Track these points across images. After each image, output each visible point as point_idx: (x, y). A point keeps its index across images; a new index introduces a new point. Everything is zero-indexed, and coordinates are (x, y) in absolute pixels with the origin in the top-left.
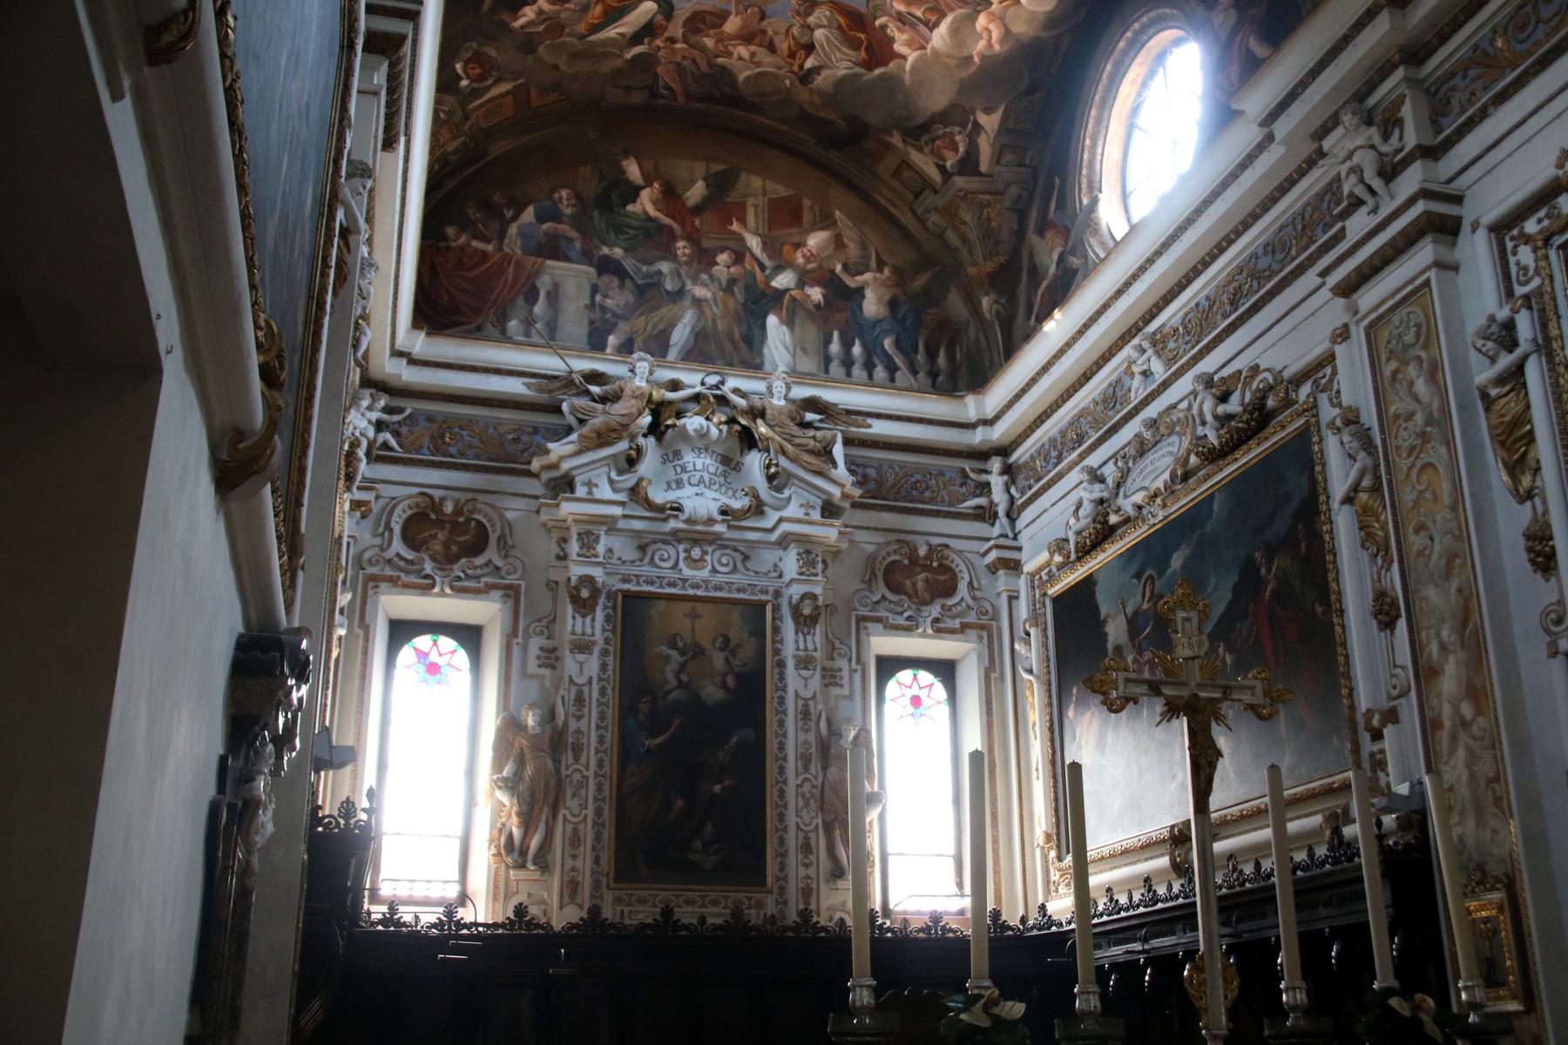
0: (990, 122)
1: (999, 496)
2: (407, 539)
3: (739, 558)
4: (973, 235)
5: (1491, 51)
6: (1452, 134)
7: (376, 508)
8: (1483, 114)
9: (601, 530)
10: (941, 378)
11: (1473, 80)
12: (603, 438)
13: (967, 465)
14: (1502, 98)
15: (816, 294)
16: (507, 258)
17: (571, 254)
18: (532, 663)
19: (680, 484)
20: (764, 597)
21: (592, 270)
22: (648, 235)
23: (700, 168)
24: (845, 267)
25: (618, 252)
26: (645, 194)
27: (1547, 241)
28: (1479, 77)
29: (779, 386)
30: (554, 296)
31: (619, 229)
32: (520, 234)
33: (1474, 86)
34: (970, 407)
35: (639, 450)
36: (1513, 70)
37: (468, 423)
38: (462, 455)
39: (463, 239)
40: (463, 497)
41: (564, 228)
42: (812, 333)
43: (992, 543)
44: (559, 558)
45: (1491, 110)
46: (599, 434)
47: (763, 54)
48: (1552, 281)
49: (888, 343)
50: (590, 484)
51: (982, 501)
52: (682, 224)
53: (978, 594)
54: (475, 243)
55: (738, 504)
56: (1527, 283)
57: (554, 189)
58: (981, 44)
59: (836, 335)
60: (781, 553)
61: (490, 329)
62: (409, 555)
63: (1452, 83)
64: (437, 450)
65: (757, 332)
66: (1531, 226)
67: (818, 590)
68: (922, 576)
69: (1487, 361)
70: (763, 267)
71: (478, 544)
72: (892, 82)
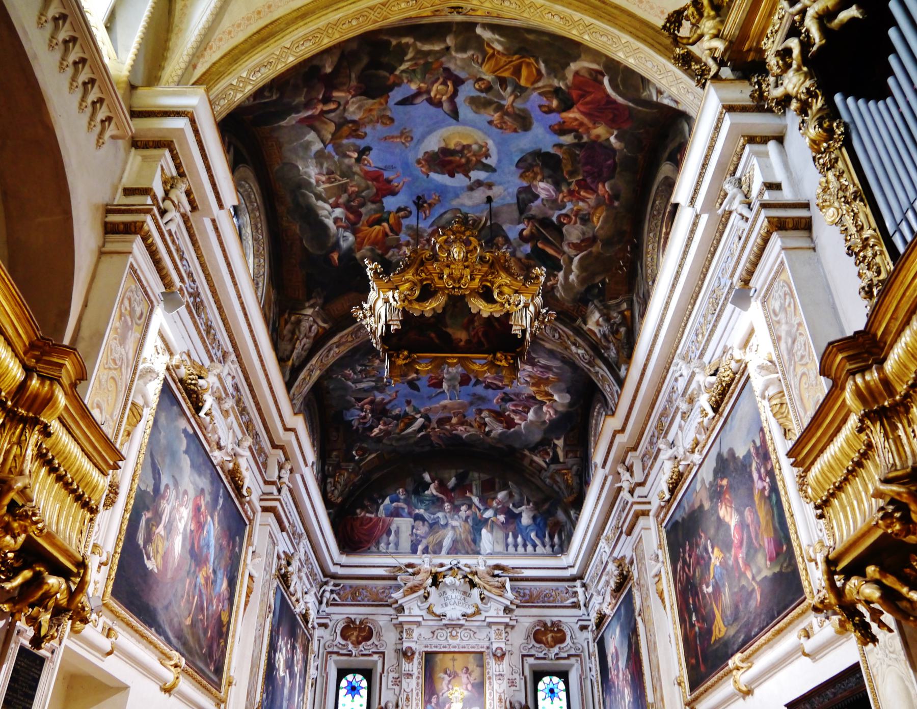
0: (560, 443)
1: (581, 598)
2: (344, 636)
3: (472, 633)
4: (563, 486)
7: (331, 624)
9: (414, 627)
10: (556, 547)
12: (413, 590)
13: (566, 584)
15: (502, 518)
16: (380, 519)
17: (404, 514)
18: (390, 684)
19: (446, 605)
20: (482, 650)
21: (412, 520)
22: (433, 503)
23: (453, 472)
24: (514, 505)
25: (422, 511)
26: (432, 486)
29: (481, 562)
30: (397, 532)
31: (422, 502)
32: (385, 509)
34: (564, 561)
35: (428, 593)
37: (365, 588)
38: (363, 600)
39: (363, 514)
40: (362, 617)
41: (401, 504)
42: (500, 534)
43: (577, 618)
44: (400, 639)
46: (411, 588)
47: (469, 428)
49: (533, 535)
50: (410, 609)
51: (575, 600)
52: (447, 496)
53: (575, 641)
54: (368, 515)
55: (471, 611)
57: (398, 489)
58: (548, 416)
59: (511, 534)
60: (489, 630)
61: (374, 549)
62: (343, 642)
64: (353, 599)
65: (478, 537)
67: (503, 646)
68: (550, 636)
70: (479, 510)
71: (369, 637)
72: (518, 434)
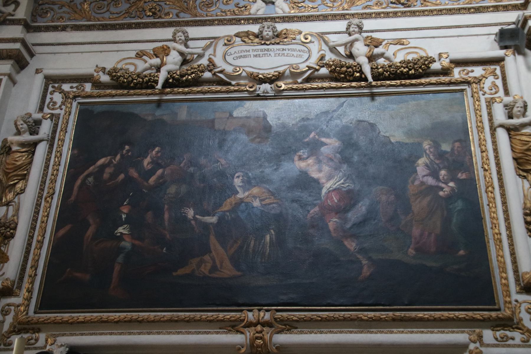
5: (79, 7)
6: (44, 26)
8: (64, 29)
11: (64, 12)
14: (77, 28)
27: (75, 97)
28: (69, 13)
33: (63, 15)
36: (88, 21)
45: (68, 29)
48: (70, 115)
56: (53, 109)
63: (52, 6)
66: (66, 87)
69: (15, 131)
